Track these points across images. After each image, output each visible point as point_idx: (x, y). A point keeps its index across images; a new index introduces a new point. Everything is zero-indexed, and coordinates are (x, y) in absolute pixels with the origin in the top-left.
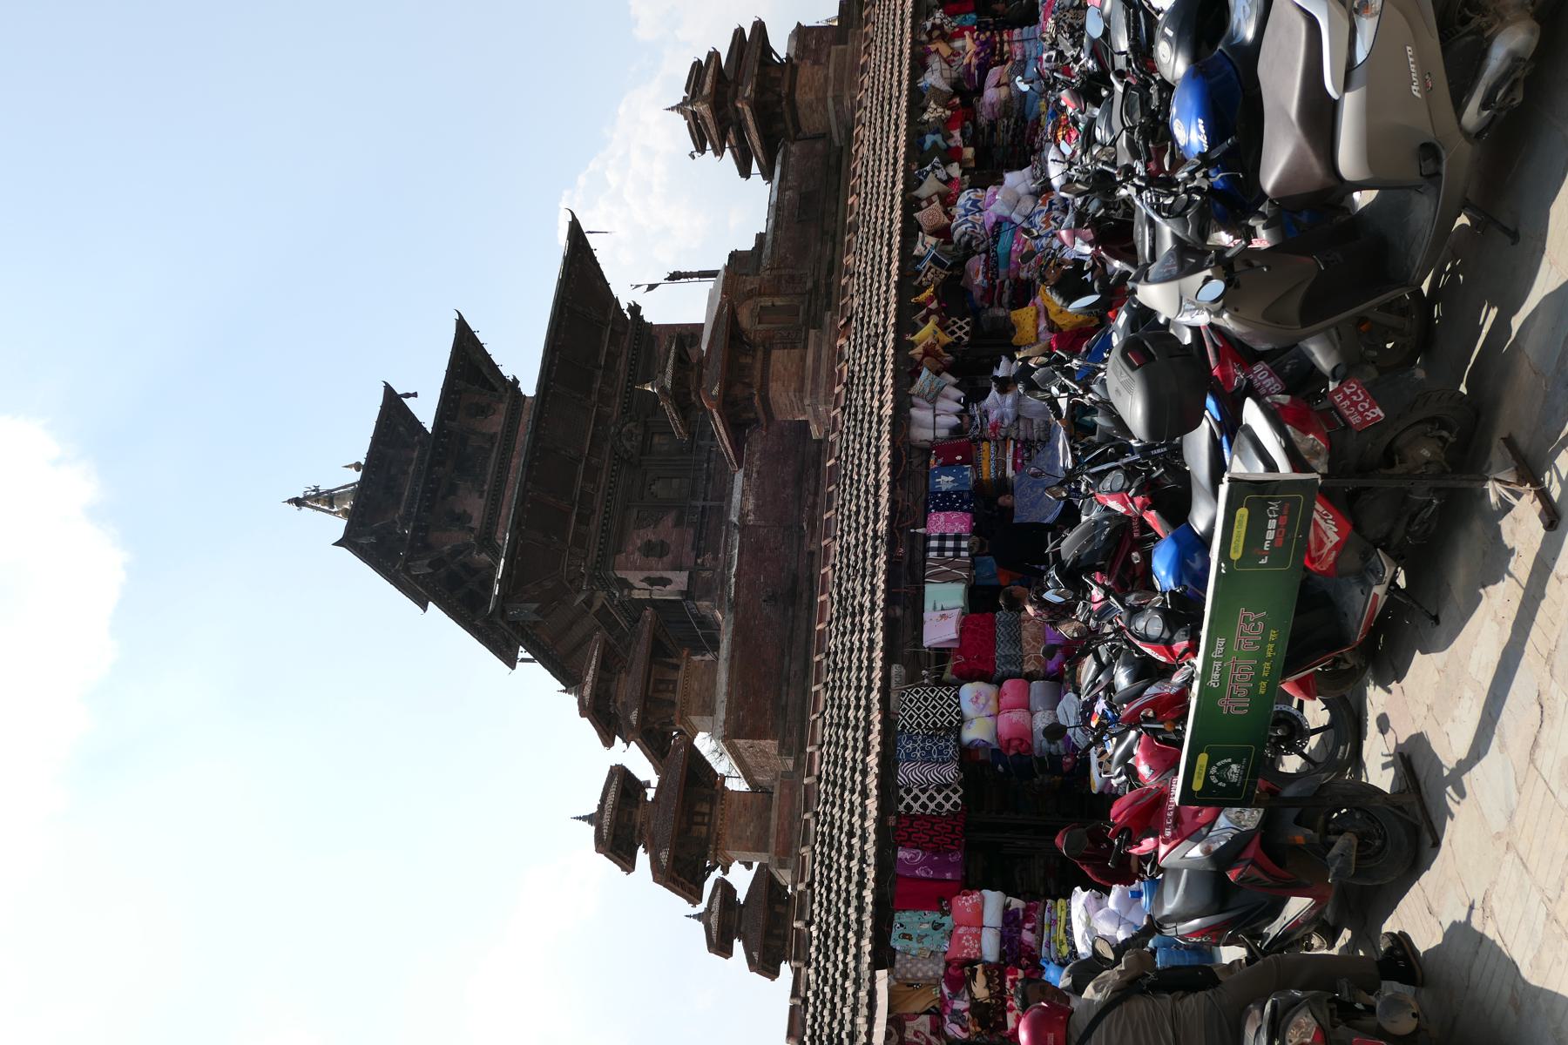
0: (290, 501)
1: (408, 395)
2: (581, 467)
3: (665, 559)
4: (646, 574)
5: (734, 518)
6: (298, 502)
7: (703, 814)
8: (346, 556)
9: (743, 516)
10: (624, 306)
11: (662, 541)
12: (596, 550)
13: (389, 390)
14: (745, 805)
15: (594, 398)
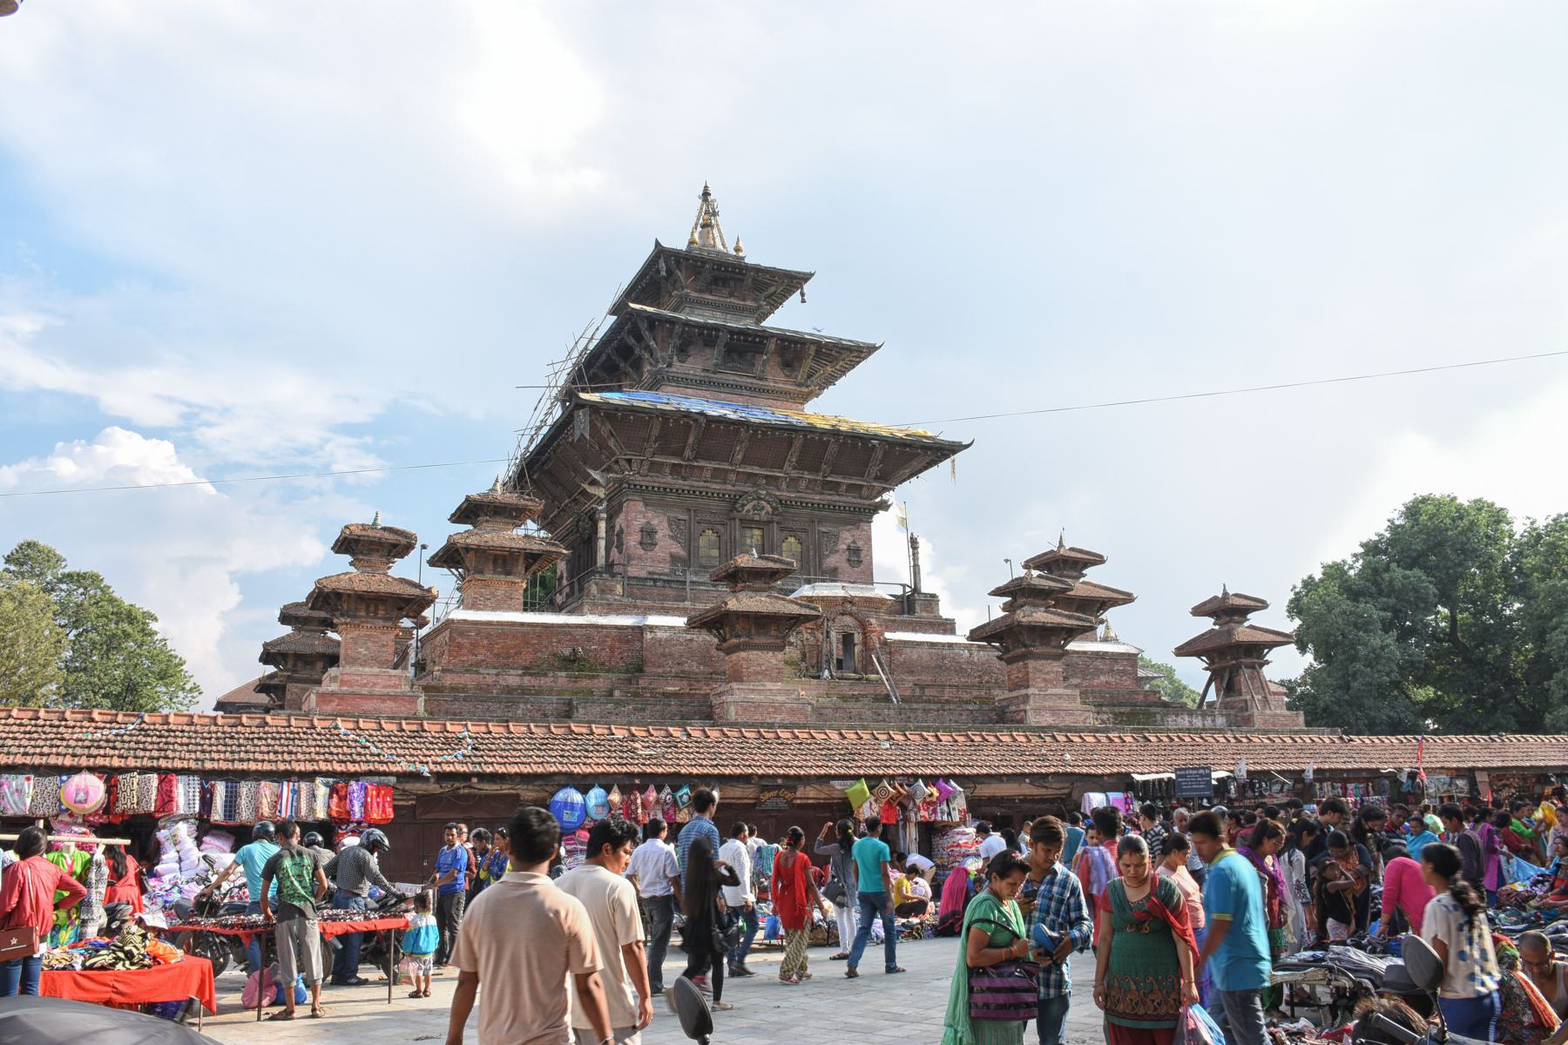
0: (706, 187)
1: (803, 294)
2: (726, 466)
3: (639, 546)
4: (625, 529)
5: (653, 620)
6: (706, 194)
7: (376, 613)
8: (647, 251)
9: (652, 628)
10: (885, 496)
11: (656, 545)
12: (647, 484)
13: (806, 277)
14: (383, 646)
15: (794, 474)
